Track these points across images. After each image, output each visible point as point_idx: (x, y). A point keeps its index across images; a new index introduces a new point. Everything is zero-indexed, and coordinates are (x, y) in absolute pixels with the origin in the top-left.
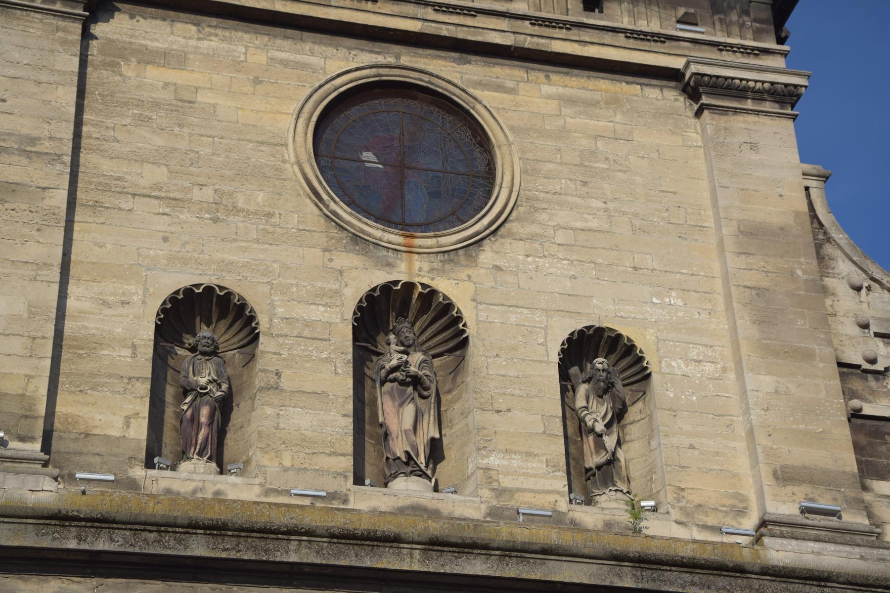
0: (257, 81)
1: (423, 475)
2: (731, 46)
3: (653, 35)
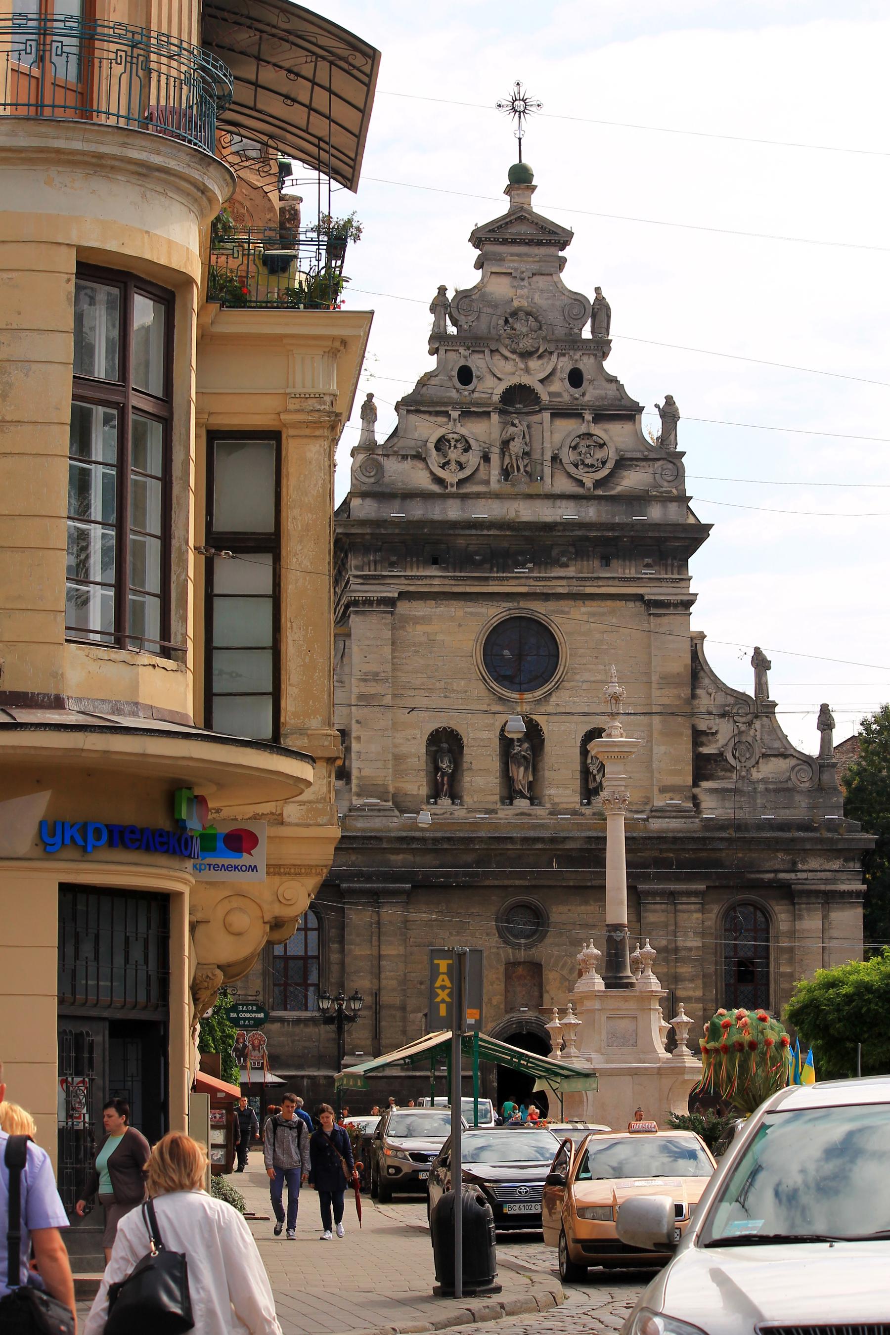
0: (460, 625)
1: (525, 797)
2: (666, 579)
3: (631, 578)
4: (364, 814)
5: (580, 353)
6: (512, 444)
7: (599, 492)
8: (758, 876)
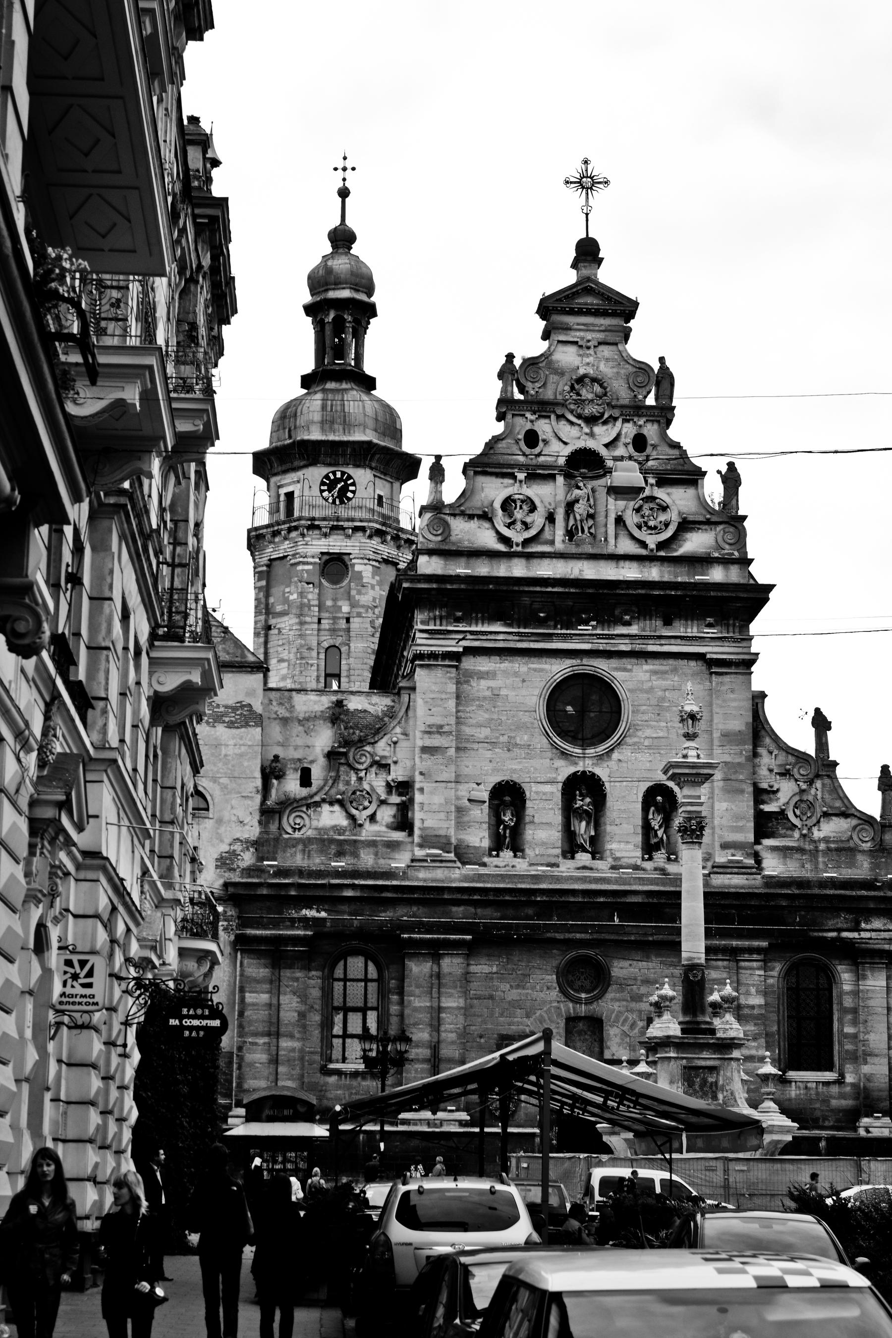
0: (524, 681)
1: (586, 851)
3: (693, 637)
4: (425, 864)
5: (644, 419)
6: (577, 506)
7: (662, 553)
8: (821, 934)
